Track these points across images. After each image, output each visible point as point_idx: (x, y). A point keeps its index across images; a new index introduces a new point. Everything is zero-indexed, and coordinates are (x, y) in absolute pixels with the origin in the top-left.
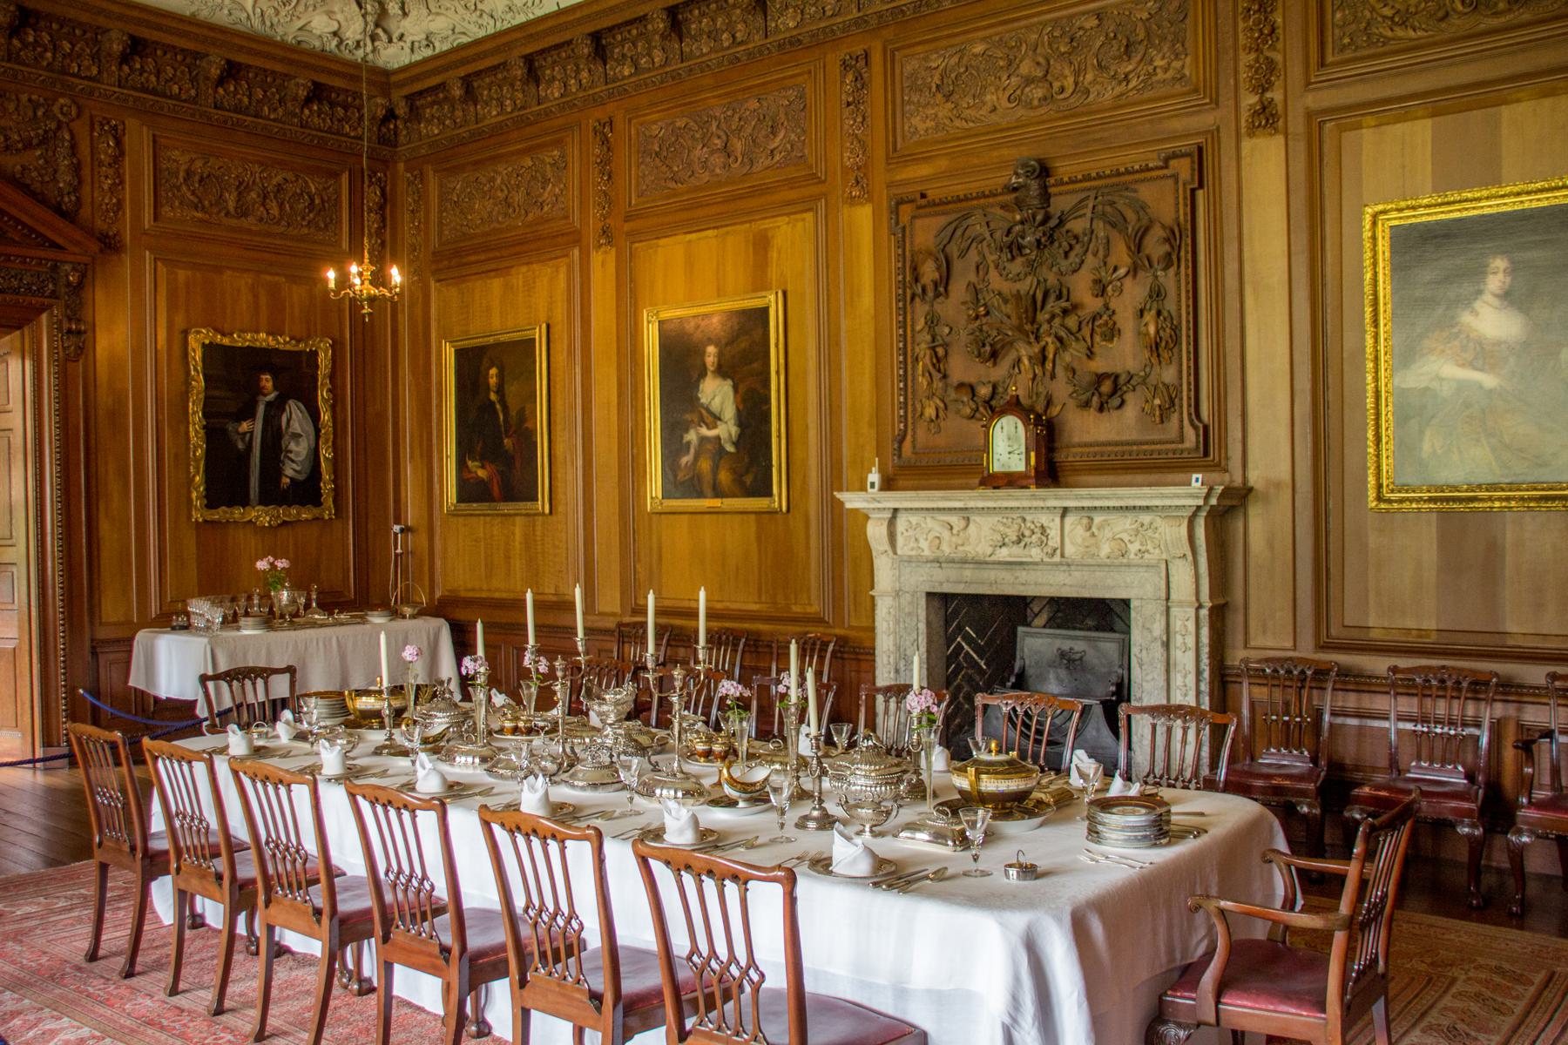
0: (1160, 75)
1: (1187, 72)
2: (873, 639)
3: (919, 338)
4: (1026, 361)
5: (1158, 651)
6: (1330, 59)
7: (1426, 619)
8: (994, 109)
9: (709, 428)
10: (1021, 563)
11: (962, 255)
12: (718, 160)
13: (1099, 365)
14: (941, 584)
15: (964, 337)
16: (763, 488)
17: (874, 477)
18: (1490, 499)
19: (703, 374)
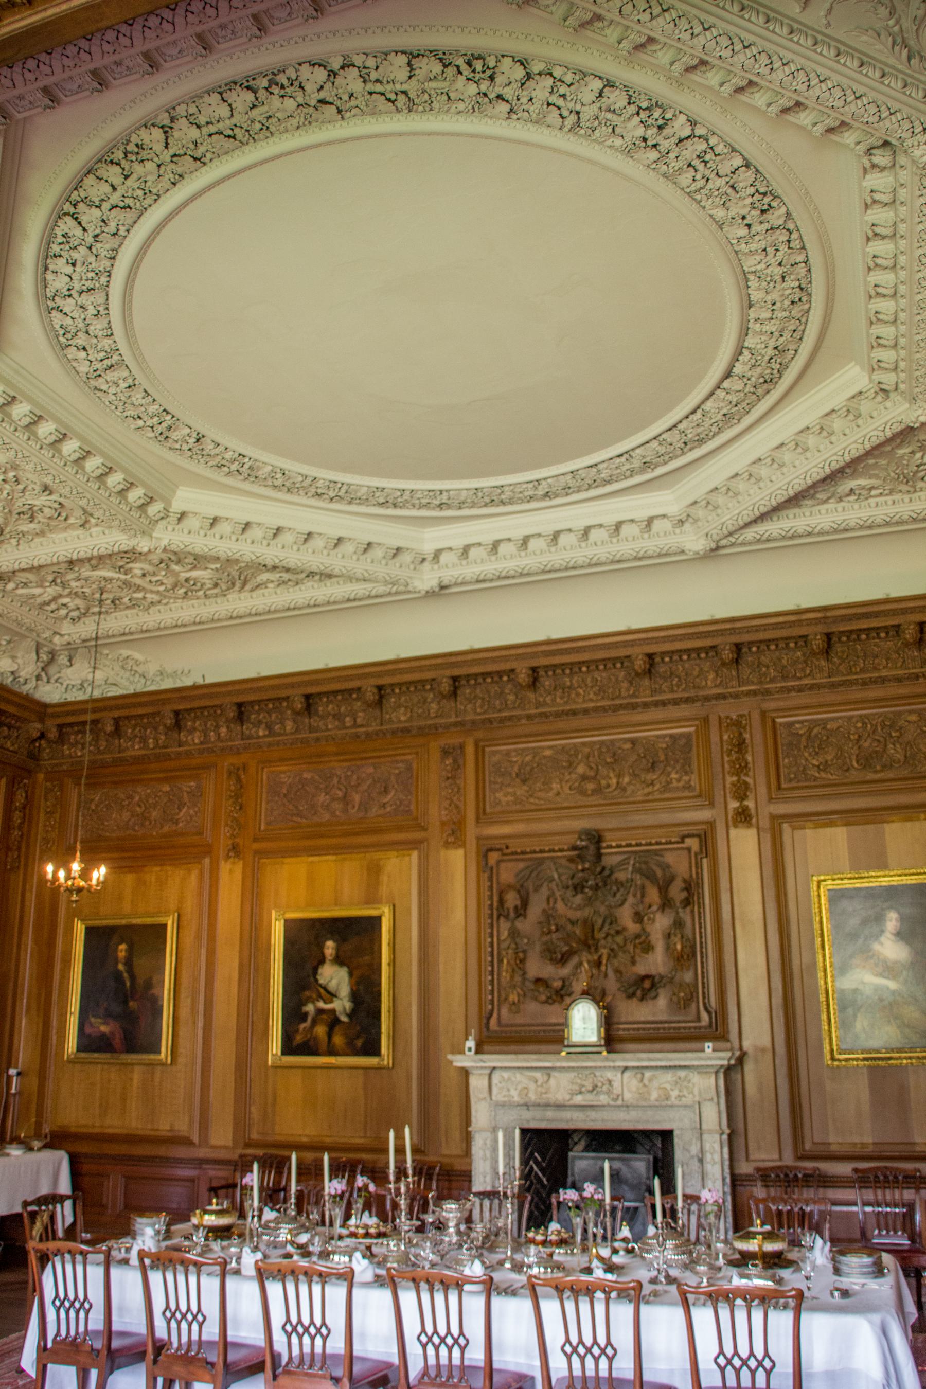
0: (675, 784)
1: (692, 783)
2: (470, 1164)
3: (504, 945)
4: (586, 965)
5: (695, 1164)
6: (783, 785)
7: (865, 1136)
8: (558, 794)
9: (325, 1002)
10: (591, 1106)
11: (537, 889)
12: (337, 806)
13: (641, 969)
14: (528, 1121)
15: (538, 947)
16: (372, 1049)
17: (471, 1043)
18: (900, 1058)
19: (322, 961)
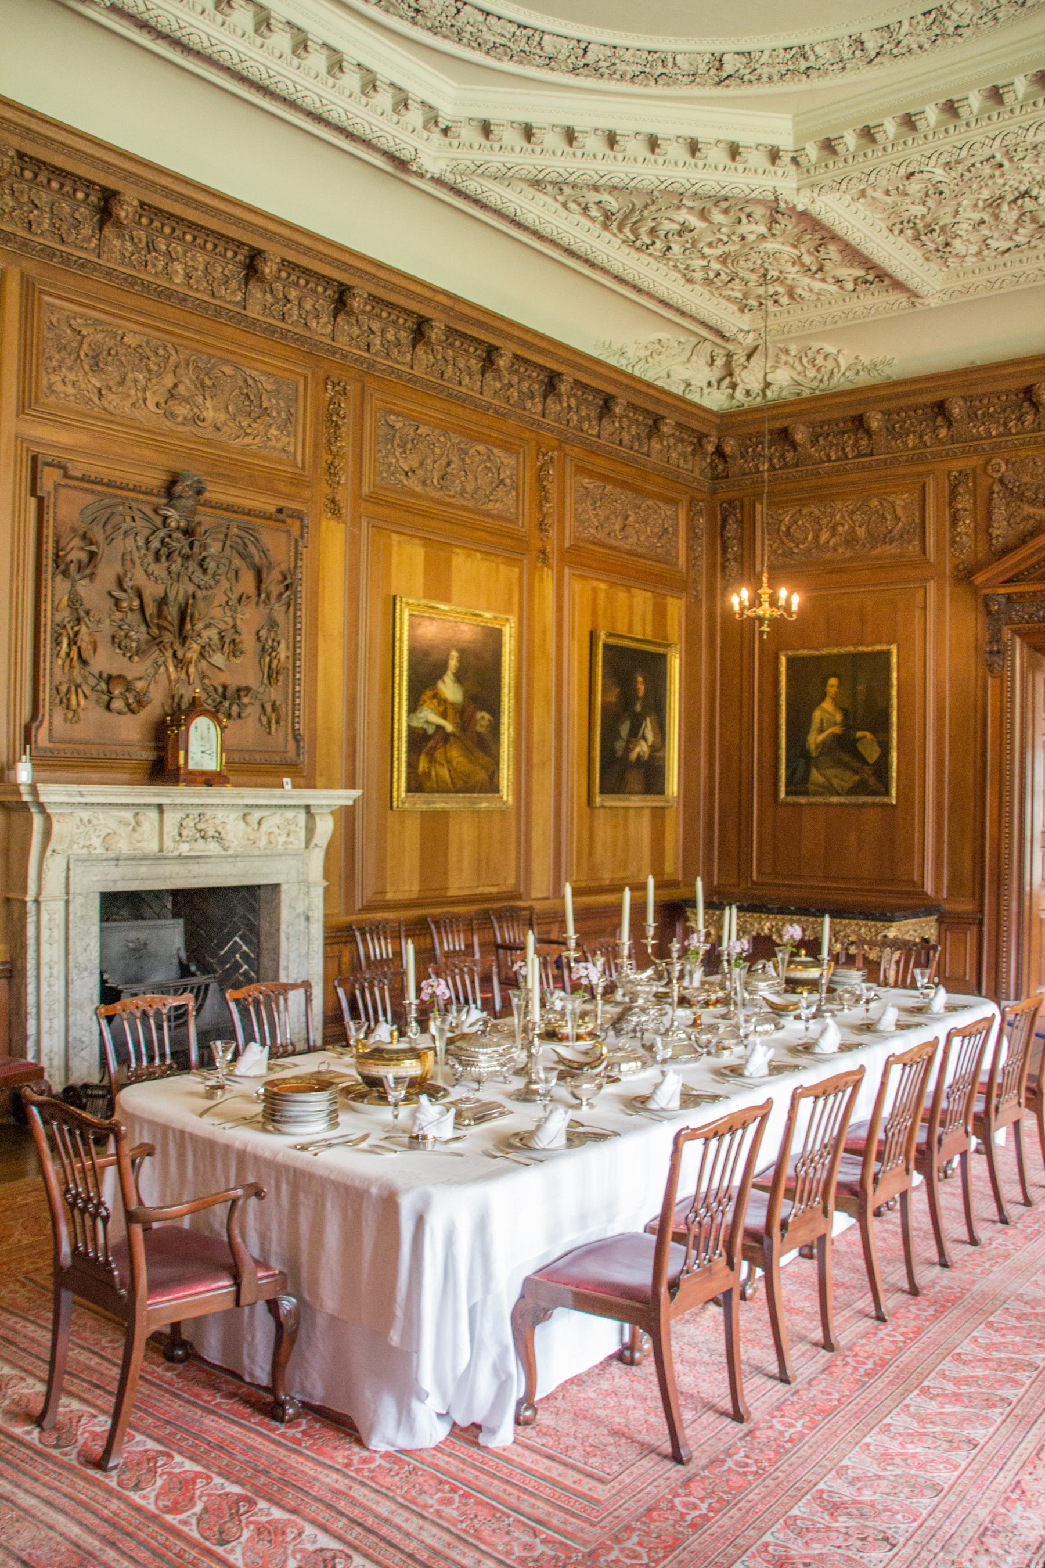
14: (115, 882)
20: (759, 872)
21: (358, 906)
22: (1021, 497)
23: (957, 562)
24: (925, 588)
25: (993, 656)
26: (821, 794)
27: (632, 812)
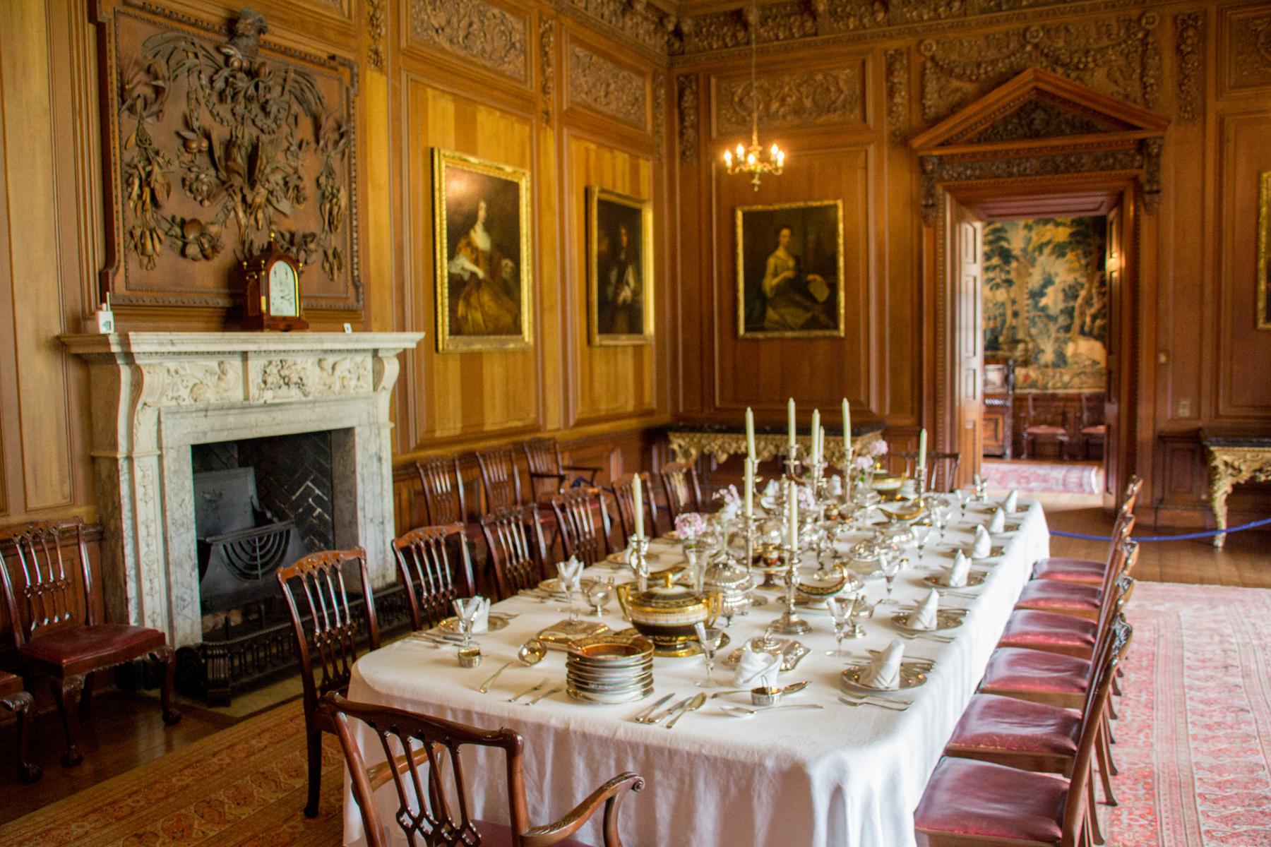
14: (205, 433)
20: (721, 399)
21: (412, 445)
22: (951, 73)
23: (893, 128)
24: (866, 152)
25: (925, 210)
26: (777, 330)
27: (619, 350)
